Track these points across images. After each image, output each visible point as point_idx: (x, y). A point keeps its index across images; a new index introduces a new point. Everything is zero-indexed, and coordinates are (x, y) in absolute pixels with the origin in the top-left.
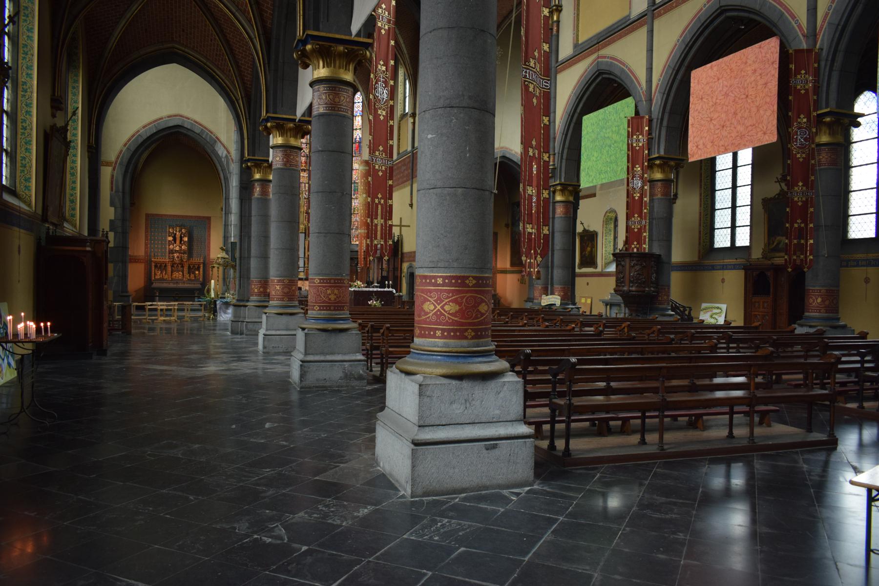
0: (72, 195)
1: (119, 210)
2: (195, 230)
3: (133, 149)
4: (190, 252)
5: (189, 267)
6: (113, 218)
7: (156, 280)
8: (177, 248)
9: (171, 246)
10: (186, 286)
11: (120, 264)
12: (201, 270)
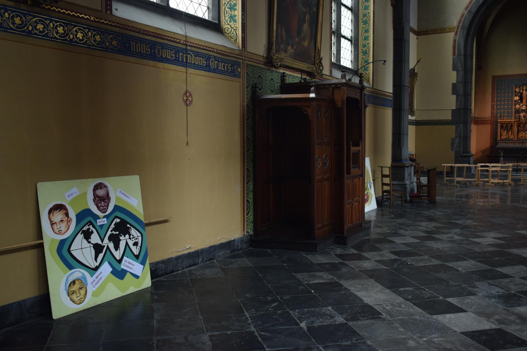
0: (364, 46)
1: (461, 73)
3: (474, 11)
6: (455, 82)
7: (501, 140)
9: (517, 106)
11: (462, 126)
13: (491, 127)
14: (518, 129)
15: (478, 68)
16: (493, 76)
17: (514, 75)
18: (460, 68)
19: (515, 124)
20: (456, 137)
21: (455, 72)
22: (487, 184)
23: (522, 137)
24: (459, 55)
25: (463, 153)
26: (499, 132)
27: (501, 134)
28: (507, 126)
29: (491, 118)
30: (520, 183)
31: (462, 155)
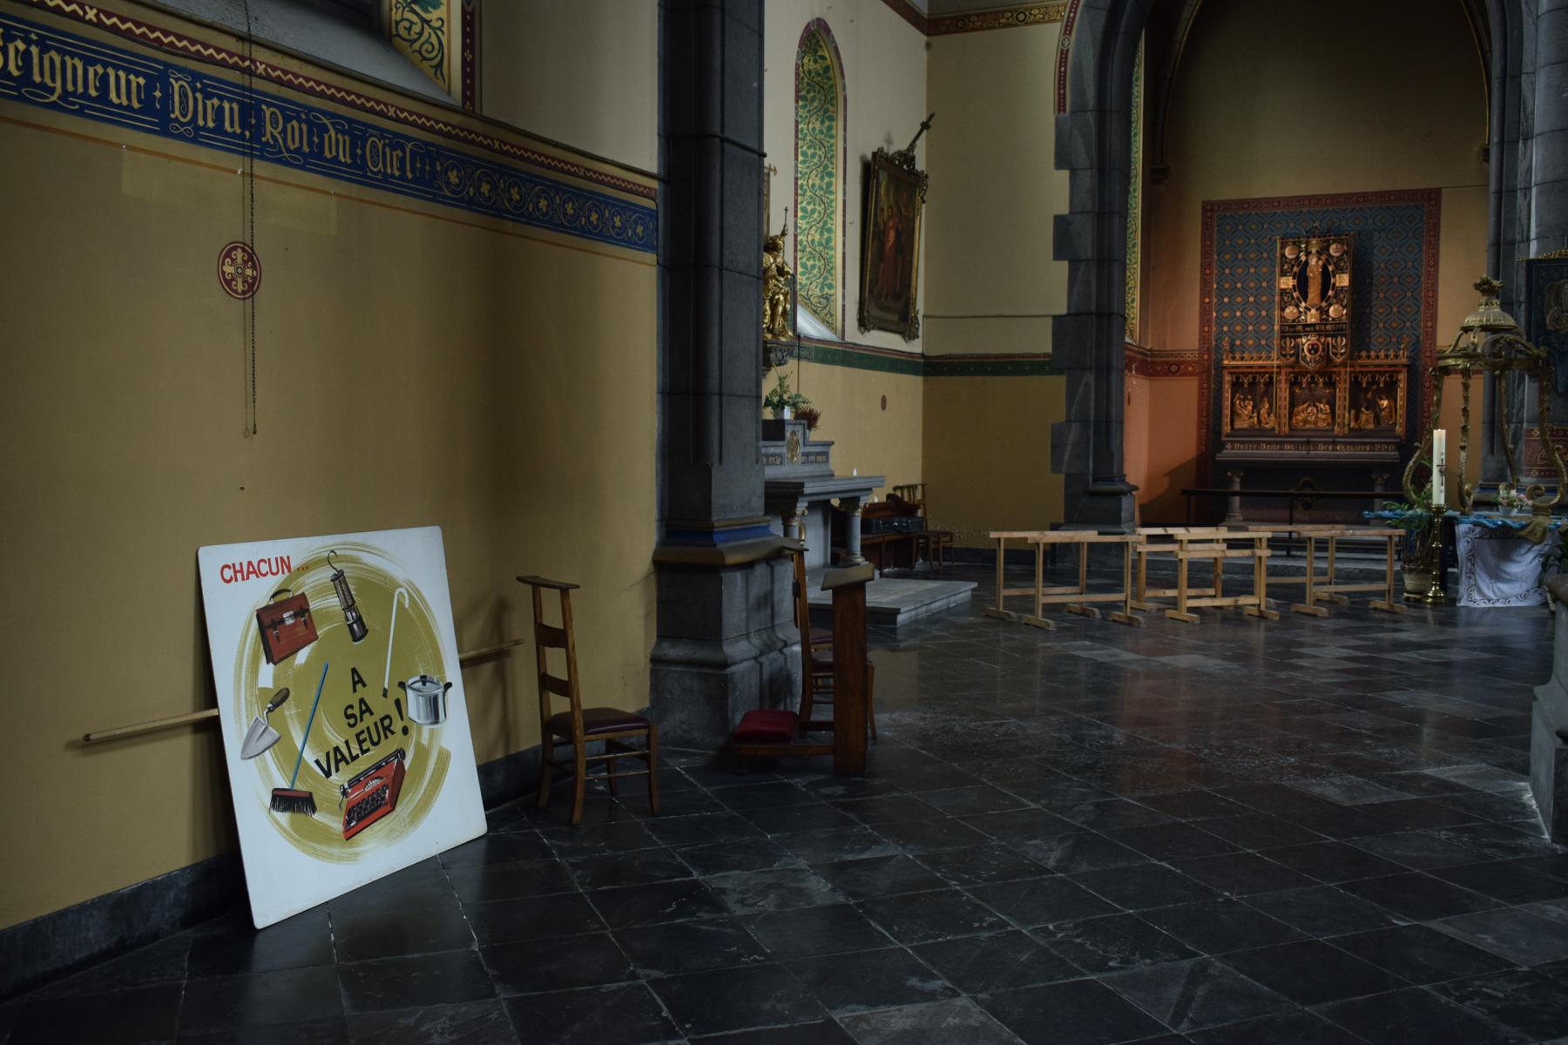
1: (1087, 179)
2: (1378, 246)
4: (1358, 328)
5: (1355, 385)
6: (1064, 209)
8: (1312, 317)
9: (1290, 312)
10: (1343, 452)
11: (1090, 378)
12: (1401, 393)
13: (1201, 388)
14: (1292, 394)
15: (1157, 174)
16: (1205, 204)
17: (1278, 200)
18: (1083, 159)
19: (1283, 377)
20: (1069, 421)
21: (1065, 174)
22: (1170, 613)
23: (1305, 421)
24: (1079, 109)
25: (1095, 480)
26: (1228, 403)
27: (1233, 412)
28: (1253, 384)
29: (1201, 355)
30: (1301, 607)
31: (1091, 487)
